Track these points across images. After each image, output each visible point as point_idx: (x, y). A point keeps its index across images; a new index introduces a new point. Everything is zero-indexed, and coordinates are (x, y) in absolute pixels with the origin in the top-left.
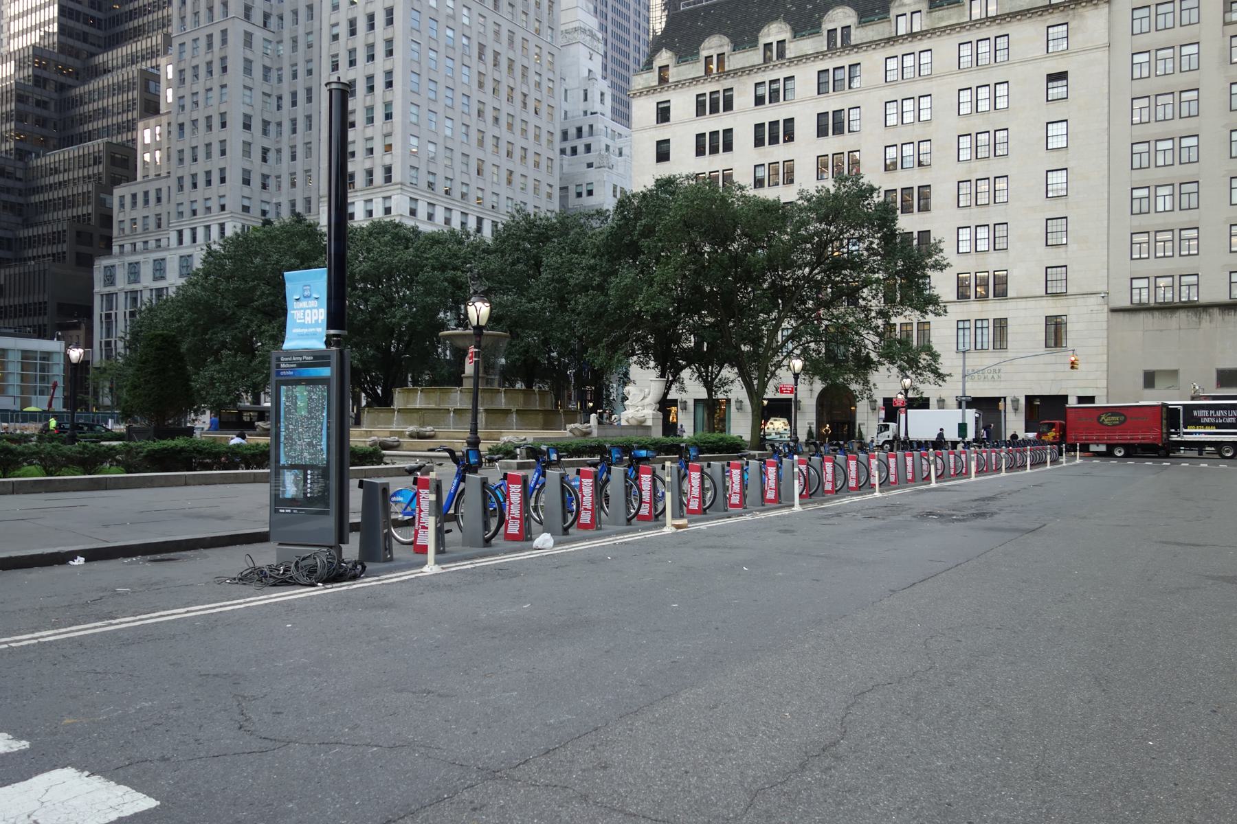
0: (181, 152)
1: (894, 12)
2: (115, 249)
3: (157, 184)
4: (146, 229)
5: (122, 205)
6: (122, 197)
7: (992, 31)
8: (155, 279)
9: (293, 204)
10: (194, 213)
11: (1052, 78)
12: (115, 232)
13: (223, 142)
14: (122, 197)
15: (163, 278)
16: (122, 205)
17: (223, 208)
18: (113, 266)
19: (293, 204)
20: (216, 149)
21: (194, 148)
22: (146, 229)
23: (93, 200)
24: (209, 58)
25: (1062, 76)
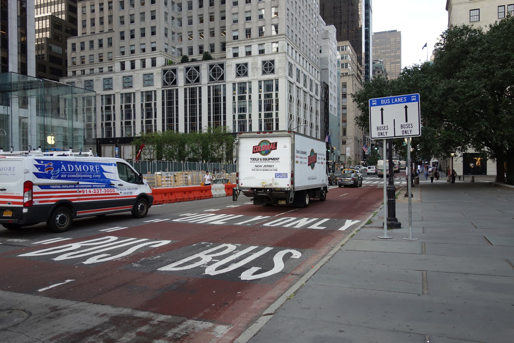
0: (122, 17)
2: (70, 73)
3: (100, 37)
4: (92, 62)
5: (74, 49)
6: (74, 45)
8: (105, 89)
9: (201, 48)
10: (133, 52)
12: (69, 63)
13: (153, 12)
14: (74, 45)
15: (111, 89)
16: (74, 49)
17: (154, 49)
18: (92, 81)
19: (201, 48)
20: (148, 16)
21: (132, 15)
22: (92, 62)
23: (45, 47)
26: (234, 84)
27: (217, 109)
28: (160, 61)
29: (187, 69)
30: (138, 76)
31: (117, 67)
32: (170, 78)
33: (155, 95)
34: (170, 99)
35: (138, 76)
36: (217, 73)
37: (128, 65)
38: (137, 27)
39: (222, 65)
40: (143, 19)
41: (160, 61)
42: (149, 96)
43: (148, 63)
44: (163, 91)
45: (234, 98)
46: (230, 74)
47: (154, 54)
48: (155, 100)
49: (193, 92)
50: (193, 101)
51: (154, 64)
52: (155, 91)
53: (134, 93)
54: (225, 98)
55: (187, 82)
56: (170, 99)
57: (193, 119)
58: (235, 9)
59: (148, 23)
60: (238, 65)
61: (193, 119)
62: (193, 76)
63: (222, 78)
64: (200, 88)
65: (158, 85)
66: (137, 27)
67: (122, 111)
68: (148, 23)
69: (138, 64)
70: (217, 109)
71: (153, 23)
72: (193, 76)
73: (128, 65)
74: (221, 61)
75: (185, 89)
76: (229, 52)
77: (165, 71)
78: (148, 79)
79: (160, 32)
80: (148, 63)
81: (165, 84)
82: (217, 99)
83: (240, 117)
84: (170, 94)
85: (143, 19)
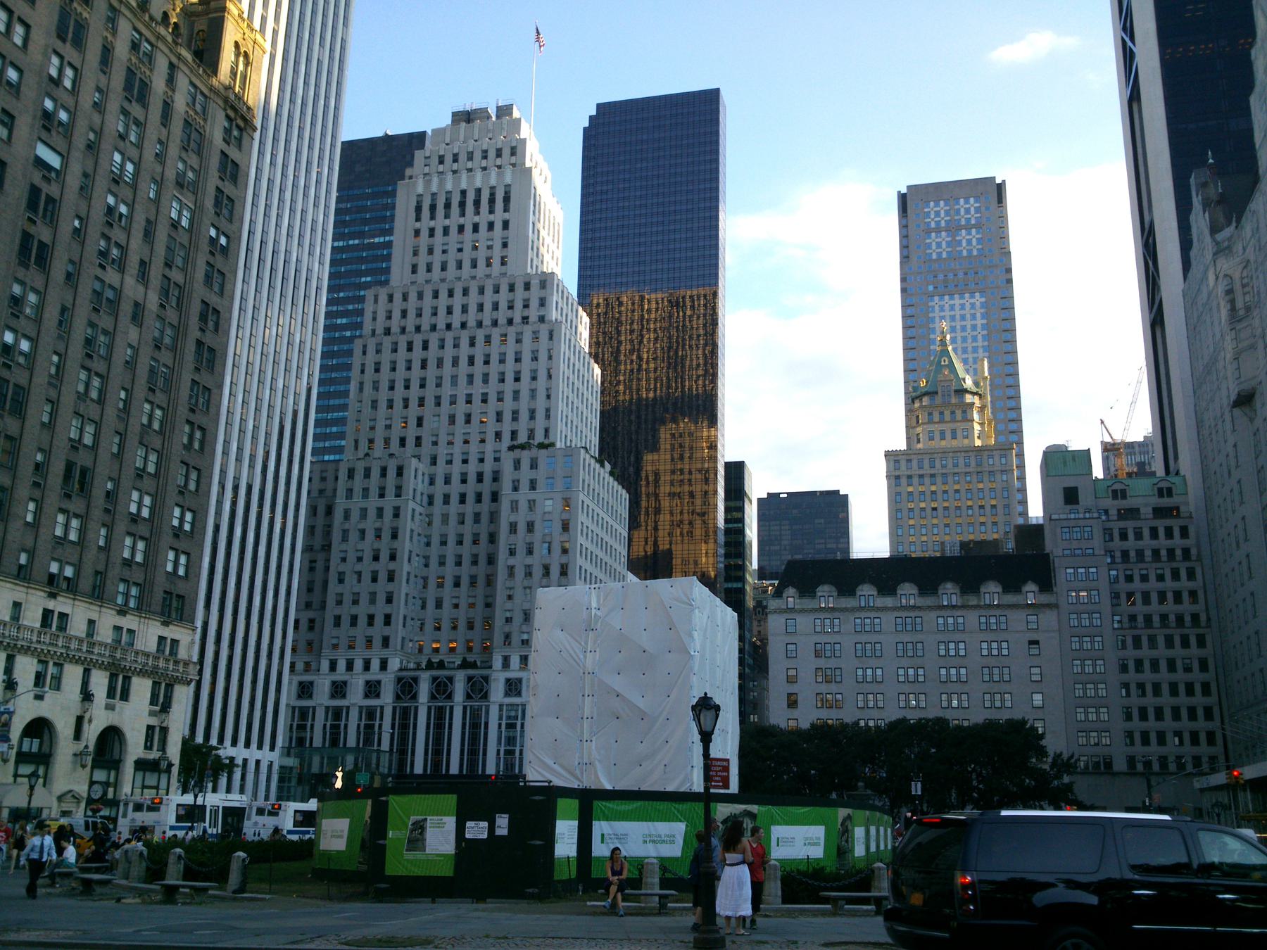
1: (940, 592)
7: (998, 612)
11: (1032, 643)
24: (378, 525)
25: (1036, 642)
26: (501, 706)
27: (474, 739)
28: (394, 664)
29: (435, 679)
30: (357, 683)
31: (325, 665)
32: (406, 688)
33: (382, 713)
34: (404, 720)
35: (357, 683)
36: (478, 689)
37: (342, 665)
38: (362, 610)
39: (486, 679)
40: (373, 601)
41: (394, 664)
42: (370, 713)
43: (375, 664)
44: (394, 708)
45: (500, 725)
46: (497, 693)
47: (385, 653)
48: (381, 719)
49: (440, 710)
50: (439, 726)
51: (384, 665)
52: (382, 707)
53: (348, 708)
54: (486, 724)
55: (433, 697)
56: (404, 720)
57: (437, 752)
58: (509, 605)
59: (380, 609)
60: (508, 680)
61: (437, 752)
62: (442, 689)
63: (485, 696)
64: (452, 708)
65: (387, 698)
66: (362, 610)
67: (325, 733)
68: (380, 609)
69: (359, 665)
70: (474, 739)
71: (388, 609)
72: (442, 689)
73: (342, 665)
74: (484, 672)
75: (429, 708)
76: (497, 662)
77: (399, 680)
78: (372, 689)
79: (398, 621)
80: (375, 664)
81: (398, 698)
82: (475, 726)
83: (508, 752)
84: (405, 713)
85: (373, 601)
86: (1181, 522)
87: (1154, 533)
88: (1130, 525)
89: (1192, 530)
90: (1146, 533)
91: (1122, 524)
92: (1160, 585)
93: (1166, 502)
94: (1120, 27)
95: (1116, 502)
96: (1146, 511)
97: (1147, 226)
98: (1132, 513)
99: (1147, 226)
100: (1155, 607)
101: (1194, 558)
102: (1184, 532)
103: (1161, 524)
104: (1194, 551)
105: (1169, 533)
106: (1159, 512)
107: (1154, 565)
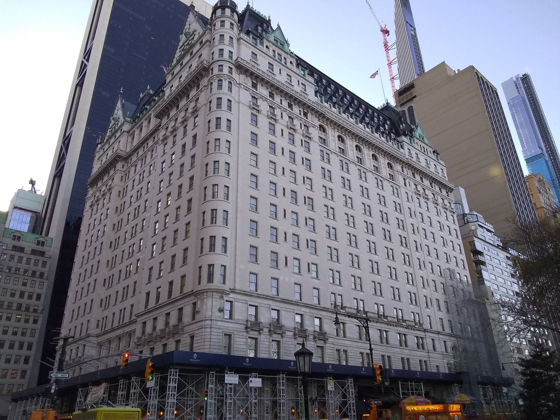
86: (44, 259)
87: (28, 261)
88: (17, 254)
89: (48, 264)
90: (24, 260)
91: (13, 253)
92: (23, 288)
93: (39, 248)
94: (82, 56)
95: (13, 241)
96: (28, 250)
97: (67, 134)
98: (22, 249)
99: (67, 134)
100: (17, 299)
101: (45, 277)
102: (44, 264)
103: (33, 257)
104: (46, 275)
105: (36, 264)
106: (34, 252)
107: (23, 277)
